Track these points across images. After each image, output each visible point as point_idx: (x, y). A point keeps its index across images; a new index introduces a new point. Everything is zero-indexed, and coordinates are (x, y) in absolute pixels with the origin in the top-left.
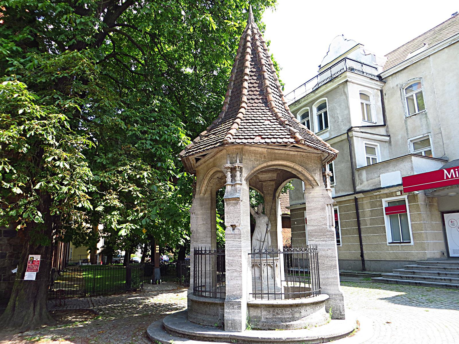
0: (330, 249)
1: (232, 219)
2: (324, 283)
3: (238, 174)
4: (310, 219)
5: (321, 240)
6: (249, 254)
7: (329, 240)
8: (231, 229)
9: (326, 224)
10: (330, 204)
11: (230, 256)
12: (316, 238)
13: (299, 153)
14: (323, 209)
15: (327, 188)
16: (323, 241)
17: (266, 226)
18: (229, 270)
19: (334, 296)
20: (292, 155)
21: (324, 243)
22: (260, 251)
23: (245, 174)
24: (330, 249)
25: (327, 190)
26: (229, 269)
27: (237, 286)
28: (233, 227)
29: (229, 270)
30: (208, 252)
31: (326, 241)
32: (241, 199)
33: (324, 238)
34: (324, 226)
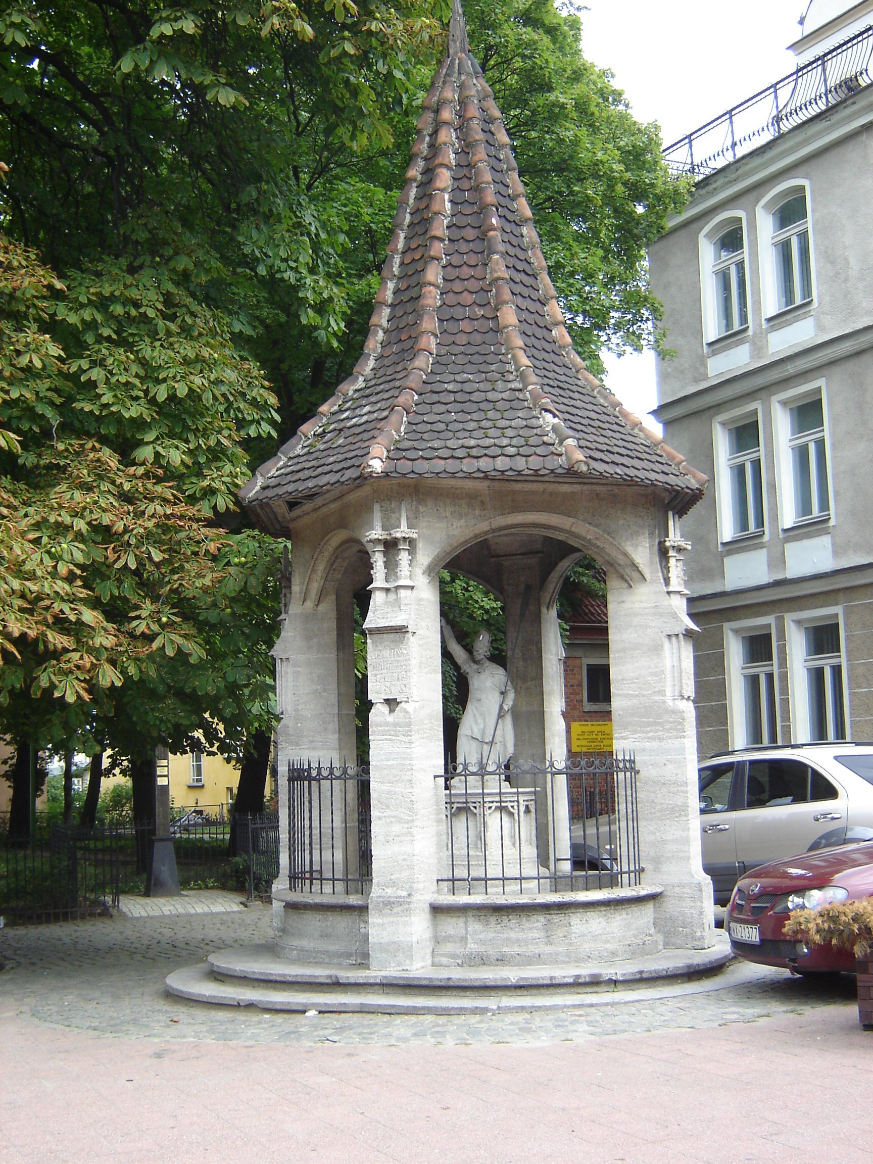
0: (670, 761)
1: (388, 684)
2: (652, 854)
3: (404, 557)
4: (620, 677)
5: (649, 738)
6: (435, 777)
7: (670, 738)
8: (385, 709)
9: (662, 692)
10: (677, 635)
11: (382, 783)
12: (635, 732)
13: (586, 487)
14: (656, 649)
15: (671, 589)
16: (654, 738)
18: (380, 818)
19: (677, 889)
20: (565, 495)
21: (655, 744)
22: (482, 767)
23: (424, 557)
24: (670, 761)
25: (669, 593)
26: (380, 815)
27: (400, 857)
28: (391, 703)
29: (380, 818)
30: (325, 773)
31: (660, 739)
32: (410, 629)
33: (657, 731)
34: (657, 698)
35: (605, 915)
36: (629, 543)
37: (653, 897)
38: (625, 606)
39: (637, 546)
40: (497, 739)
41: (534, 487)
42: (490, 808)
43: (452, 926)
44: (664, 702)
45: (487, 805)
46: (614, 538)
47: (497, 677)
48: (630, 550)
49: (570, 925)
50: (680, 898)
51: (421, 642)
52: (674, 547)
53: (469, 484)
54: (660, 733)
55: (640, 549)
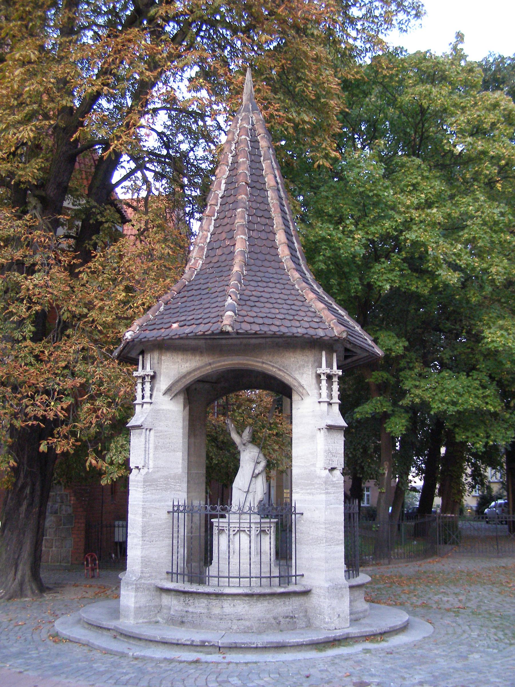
2: (307, 566)
3: (147, 386)
7: (317, 493)
9: (314, 465)
12: (302, 489)
13: (268, 340)
14: (313, 437)
15: (321, 400)
16: (309, 494)
17: (252, 465)
19: (318, 590)
21: (310, 497)
23: (163, 384)
25: (319, 402)
31: (313, 494)
32: (145, 426)
33: (311, 489)
34: (312, 468)
35: (249, 603)
36: (297, 372)
37: (306, 593)
38: (300, 411)
39: (303, 374)
40: (250, 490)
41: (238, 341)
42: (234, 531)
43: (166, 600)
45: (232, 529)
46: (287, 370)
47: (252, 453)
48: (297, 376)
49: (223, 607)
50: (319, 596)
51: (158, 434)
53: (193, 342)
54: (313, 491)
55: (305, 376)
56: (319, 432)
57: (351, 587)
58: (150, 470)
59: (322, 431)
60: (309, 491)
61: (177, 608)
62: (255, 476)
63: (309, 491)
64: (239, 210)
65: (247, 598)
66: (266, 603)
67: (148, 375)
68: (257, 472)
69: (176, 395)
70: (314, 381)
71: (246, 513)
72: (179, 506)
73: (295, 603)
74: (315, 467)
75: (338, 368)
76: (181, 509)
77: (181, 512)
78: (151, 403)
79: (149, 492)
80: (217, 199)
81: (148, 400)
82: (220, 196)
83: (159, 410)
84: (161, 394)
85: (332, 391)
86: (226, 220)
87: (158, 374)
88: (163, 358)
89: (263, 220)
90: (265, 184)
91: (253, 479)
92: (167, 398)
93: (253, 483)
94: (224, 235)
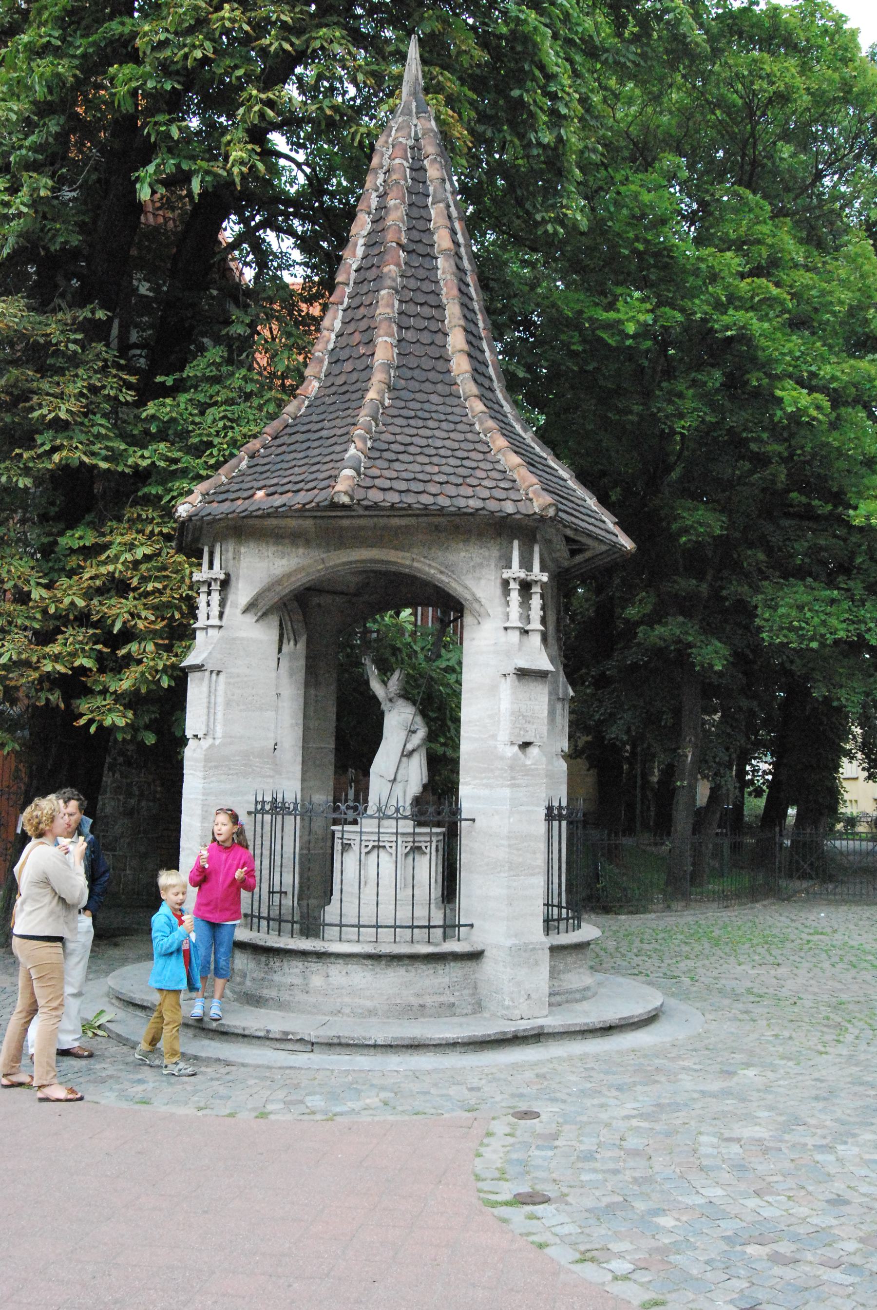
9: (494, 737)
13: (421, 519)
14: (493, 689)
15: (507, 625)
16: (486, 786)
17: (403, 735)
21: (486, 792)
25: (506, 629)
32: (209, 667)
35: (373, 970)
36: (470, 576)
37: (475, 956)
39: (480, 579)
40: (399, 778)
41: (368, 522)
42: (367, 846)
44: (496, 747)
45: (364, 843)
46: (453, 572)
47: (403, 715)
48: (470, 583)
52: (514, 579)
53: (292, 523)
54: (491, 781)
55: (483, 582)
56: (503, 679)
57: (554, 950)
58: (217, 742)
59: (508, 677)
60: (485, 781)
61: (255, 975)
62: (407, 755)
63: (485, 781)
64: (383, 292)
65: (368, 962)
66: (402, 971)
67: (215, 580)
68: (410, 747)
69: (265, 614)
70: (498, 591)
71: (389, 817)
72: (263, 802)
73: (453, 972)
74: (496, 740)
75: (542, 570)
76: (267, 807)
77: (267, 812)
78: (220, 627)
79: (214, 779)
80: (349, 274)
81: (215, 621)
82: (354, 267)
83: (234, 639)
84: (239, 611)
85: (530, 609)
86: (362, 311)
87: (233, 578)
88: (243, 550)
89: (426, 311)
90: (432, 246)
91: (404, 759)
92: (250, 618)
93: (403, 765)
94: (357, 337)
